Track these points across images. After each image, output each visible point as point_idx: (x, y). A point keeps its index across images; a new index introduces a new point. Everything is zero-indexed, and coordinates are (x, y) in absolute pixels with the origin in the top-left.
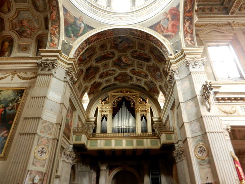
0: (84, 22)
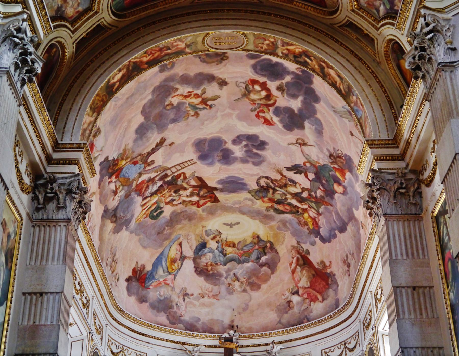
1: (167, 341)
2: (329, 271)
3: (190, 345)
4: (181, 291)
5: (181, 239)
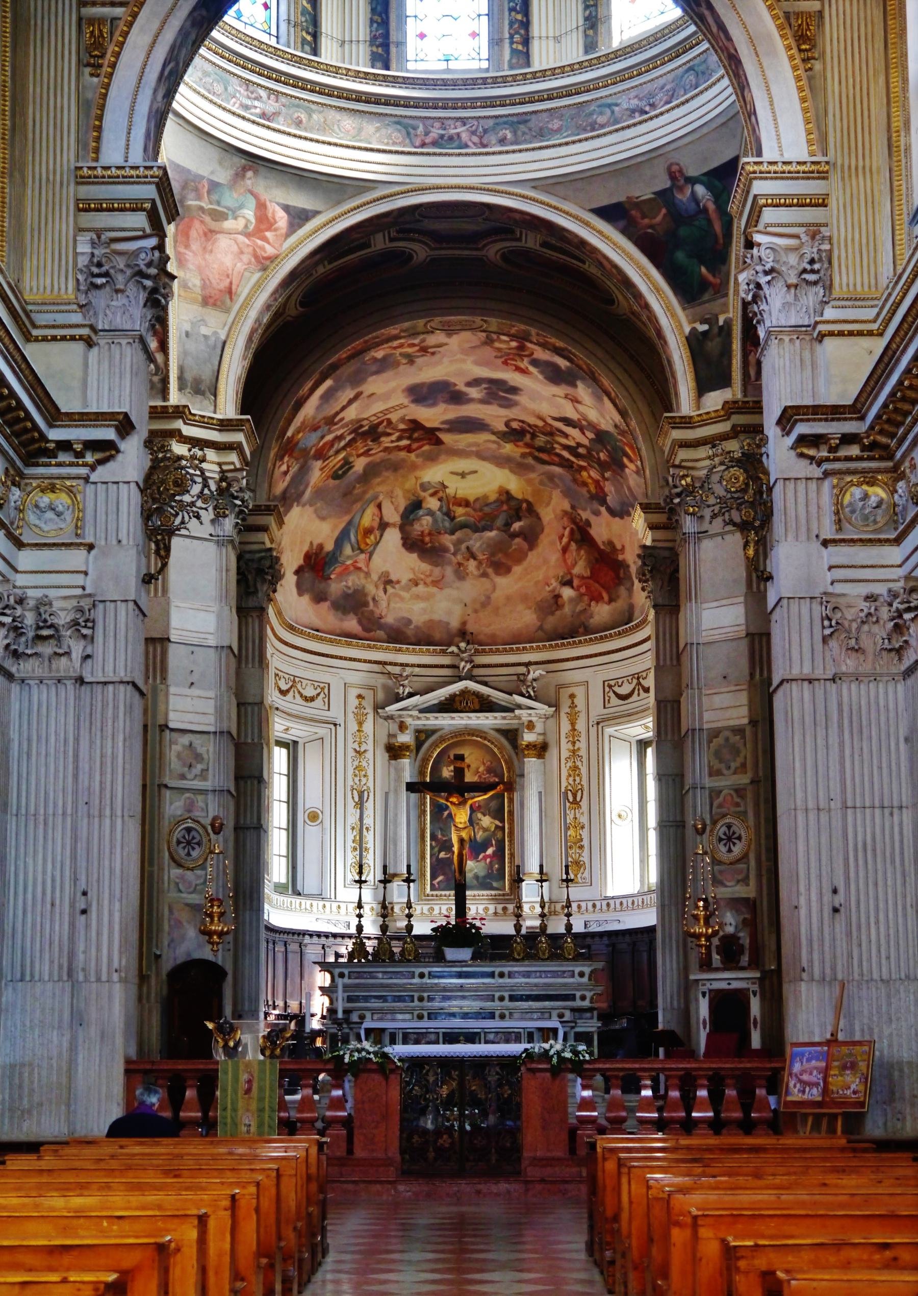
0: (692, 172)
1: (359, 660)
2: (620, 557)
3: (396, 664)
4: (380, 578)
5: (381, 497)
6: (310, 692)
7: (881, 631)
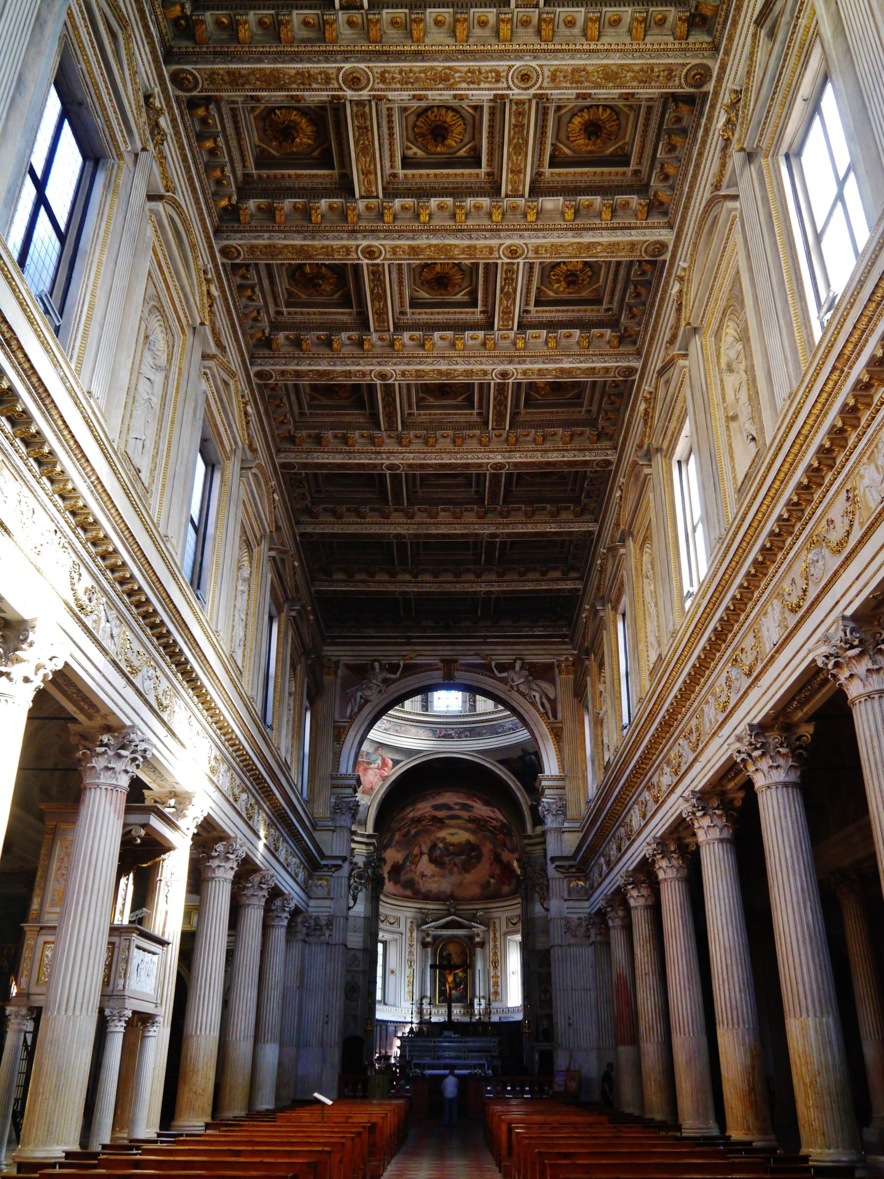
0: (531, 750)
6: (392, 921)
7: (583, 929)
